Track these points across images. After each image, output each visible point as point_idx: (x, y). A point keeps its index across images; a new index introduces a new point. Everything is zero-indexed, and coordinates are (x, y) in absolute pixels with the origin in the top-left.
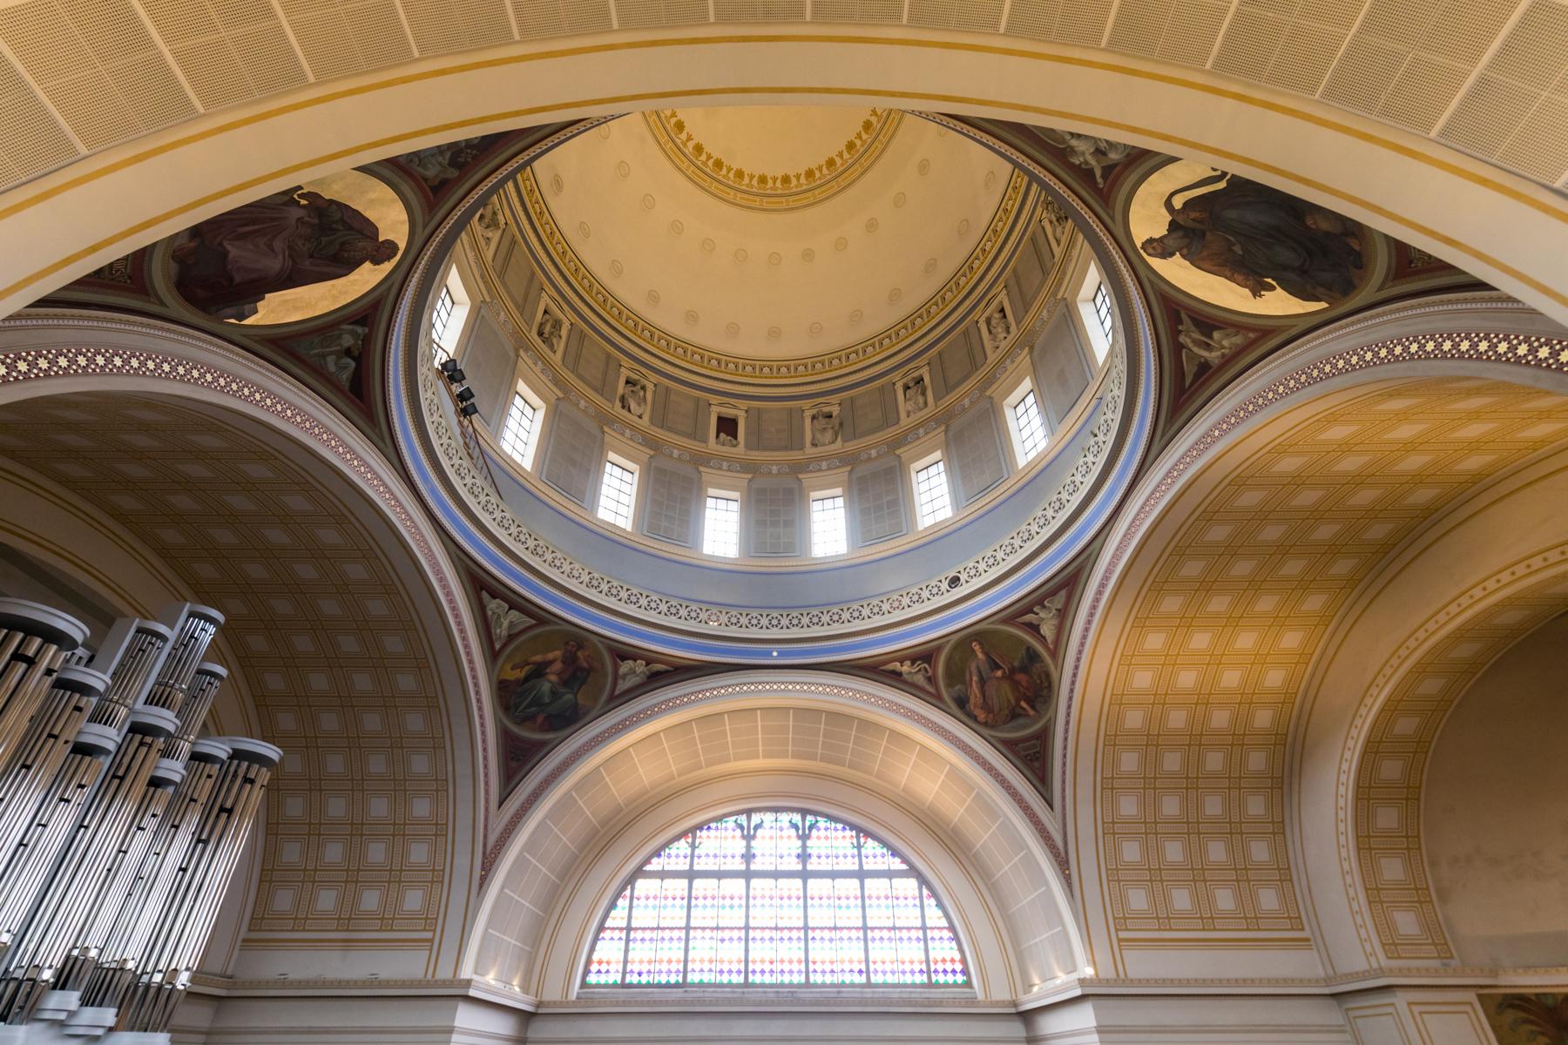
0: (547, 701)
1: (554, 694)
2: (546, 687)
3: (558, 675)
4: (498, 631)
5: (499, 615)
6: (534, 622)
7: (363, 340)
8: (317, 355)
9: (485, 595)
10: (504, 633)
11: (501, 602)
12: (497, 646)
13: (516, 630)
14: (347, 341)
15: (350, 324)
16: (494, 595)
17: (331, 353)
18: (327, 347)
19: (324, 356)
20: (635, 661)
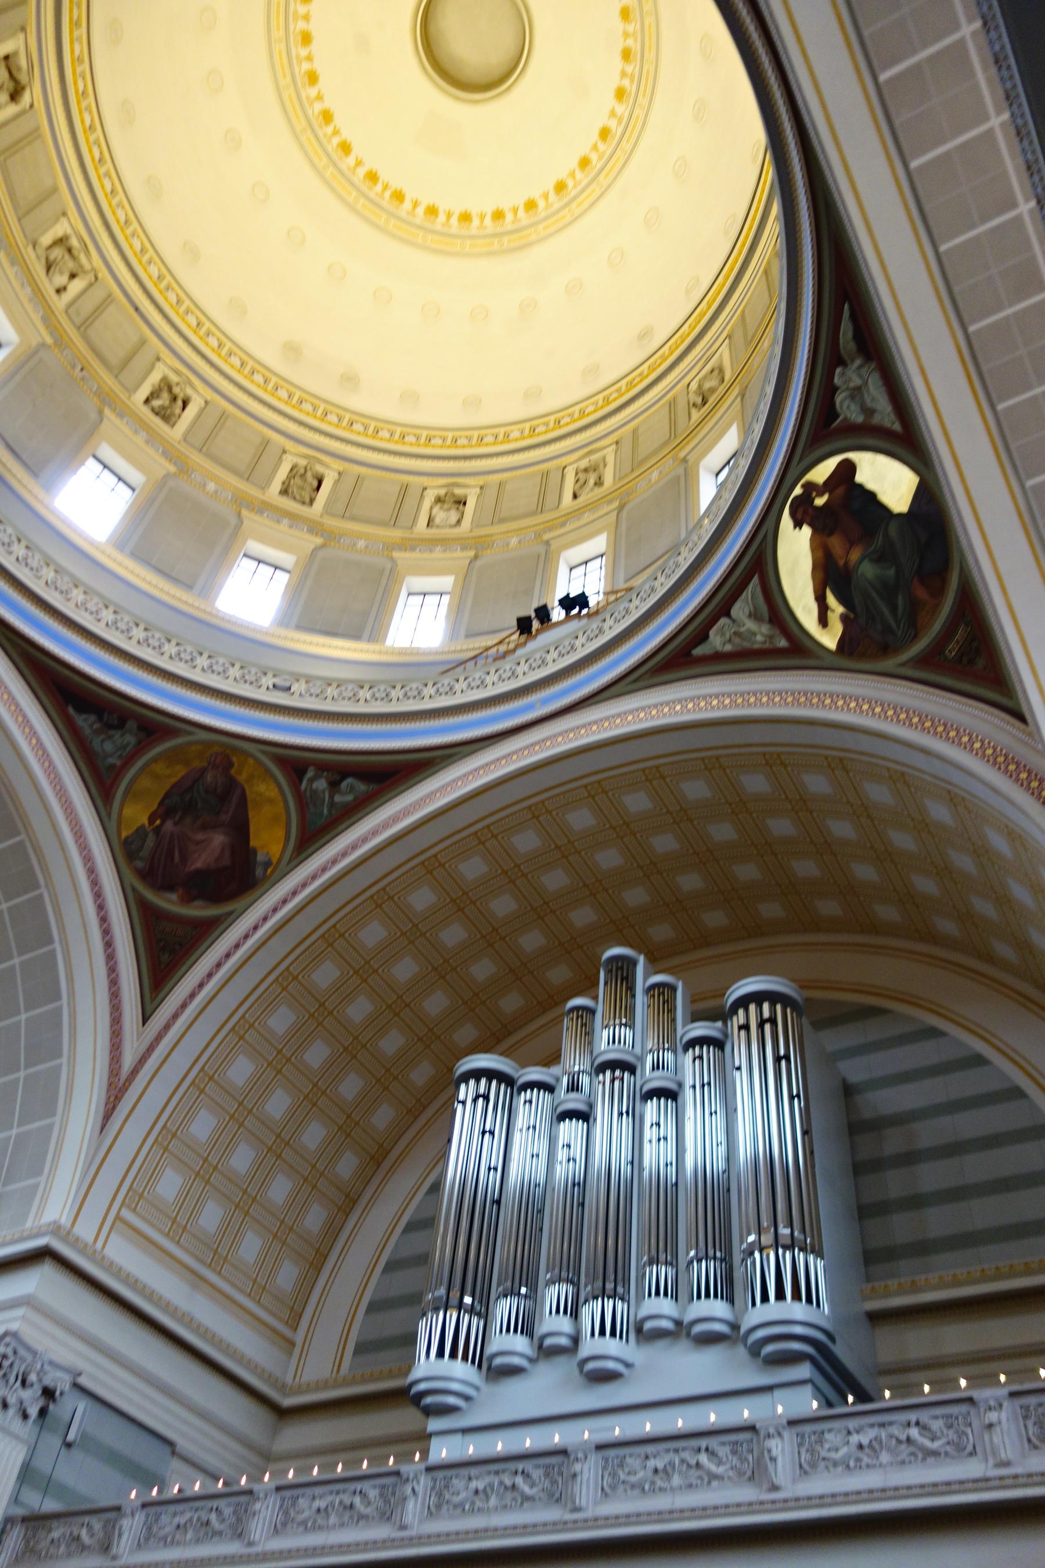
0: (892, 572)
1: (880, 558)
2: (868, 570)
3: (851, 544)
4: (759, 638)
5: (735, 633)
6: (756, 580)
7: (323, 771)
8: (330, 811)
9: (698, 651)
10: (765, 629)
11: (715, 628)
12: (783, 643)
13: (764, 609)
14: (321, 784)
15: (301, 781)
16: (702, 636)
17: (332, 797)
18: (324, 801)
19: (332, 804)
20: (835, 389)
